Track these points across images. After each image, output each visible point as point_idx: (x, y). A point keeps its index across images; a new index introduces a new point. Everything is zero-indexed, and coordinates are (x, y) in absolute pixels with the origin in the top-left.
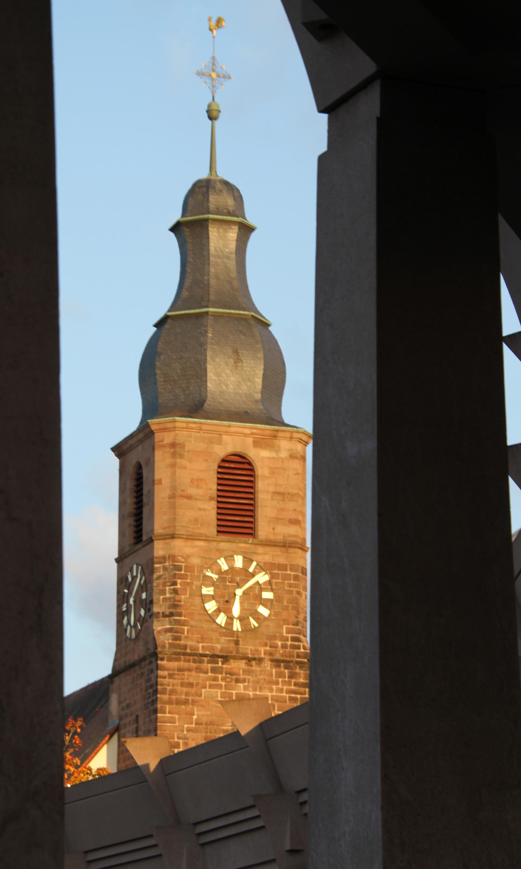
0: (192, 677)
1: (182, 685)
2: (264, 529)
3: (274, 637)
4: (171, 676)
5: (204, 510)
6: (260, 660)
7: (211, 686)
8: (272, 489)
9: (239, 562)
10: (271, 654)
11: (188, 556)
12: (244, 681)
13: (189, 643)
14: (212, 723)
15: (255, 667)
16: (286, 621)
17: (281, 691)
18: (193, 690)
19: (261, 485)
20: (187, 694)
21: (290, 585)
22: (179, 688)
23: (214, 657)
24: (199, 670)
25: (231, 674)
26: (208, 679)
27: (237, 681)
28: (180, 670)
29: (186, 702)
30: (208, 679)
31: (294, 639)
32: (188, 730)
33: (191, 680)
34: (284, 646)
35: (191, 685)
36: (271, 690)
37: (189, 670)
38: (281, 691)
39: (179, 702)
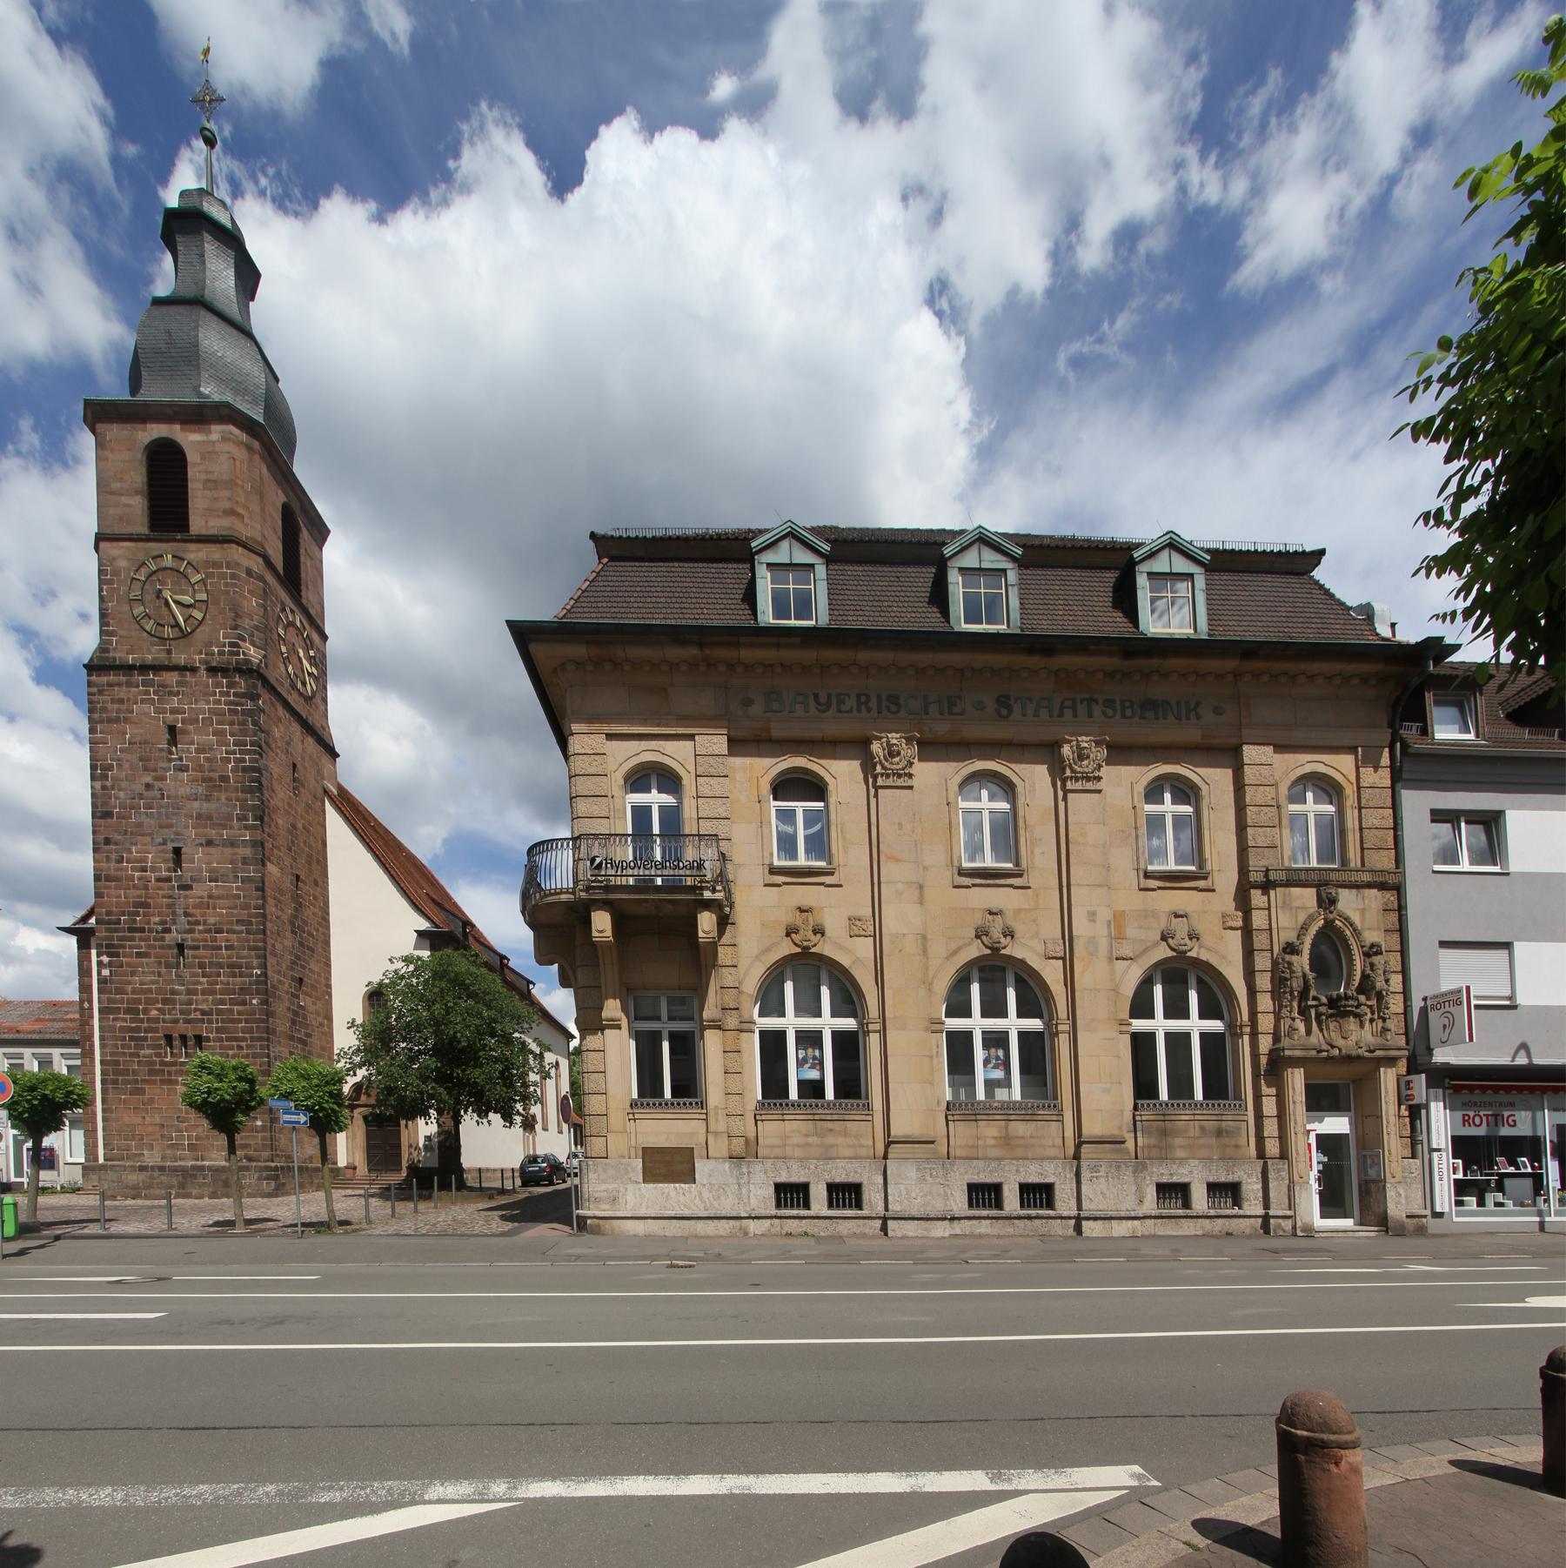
0: (122, 693)
1: (113, 701)
2: (197, 525)
3: (210, 644)
4: (100, 692)
5: (129, 506)
6: (193, 670)
7: (143, 701)
8: (203, 477)
9: (168, 561)
10: (206, 662)
11: (114, 559)
12: (178, 693)
13: (118, 655)
14: (146, 742)
15: (188, 676)
16: (223, 626)
17: (219, 702)
18: (124, 707)
19: (192, 473)
20: (118, 711)
21: (226, 585)
22: (109, 706)
23: (144, 668)
24: (129, 684)
25: (164, 686)
26: (141, 693)
27: (171, 693)
28: (110, 685)
29: (117, 720)
30: (141, 693)
31: (232, 645)
32: (122, 750)
33: (122, 695)
34: (221, 653)
35: (121, 701)
36: (208, 702)
37: (119, 685)
38: (219, 702)
39: (110, 721)
